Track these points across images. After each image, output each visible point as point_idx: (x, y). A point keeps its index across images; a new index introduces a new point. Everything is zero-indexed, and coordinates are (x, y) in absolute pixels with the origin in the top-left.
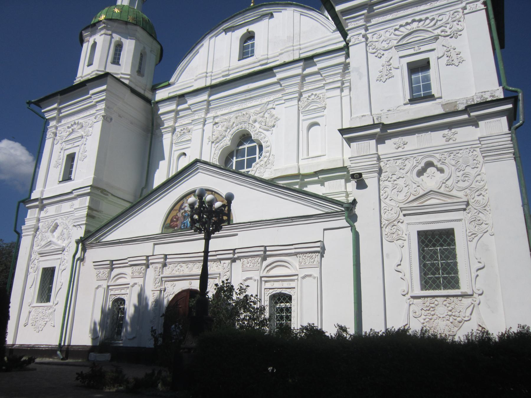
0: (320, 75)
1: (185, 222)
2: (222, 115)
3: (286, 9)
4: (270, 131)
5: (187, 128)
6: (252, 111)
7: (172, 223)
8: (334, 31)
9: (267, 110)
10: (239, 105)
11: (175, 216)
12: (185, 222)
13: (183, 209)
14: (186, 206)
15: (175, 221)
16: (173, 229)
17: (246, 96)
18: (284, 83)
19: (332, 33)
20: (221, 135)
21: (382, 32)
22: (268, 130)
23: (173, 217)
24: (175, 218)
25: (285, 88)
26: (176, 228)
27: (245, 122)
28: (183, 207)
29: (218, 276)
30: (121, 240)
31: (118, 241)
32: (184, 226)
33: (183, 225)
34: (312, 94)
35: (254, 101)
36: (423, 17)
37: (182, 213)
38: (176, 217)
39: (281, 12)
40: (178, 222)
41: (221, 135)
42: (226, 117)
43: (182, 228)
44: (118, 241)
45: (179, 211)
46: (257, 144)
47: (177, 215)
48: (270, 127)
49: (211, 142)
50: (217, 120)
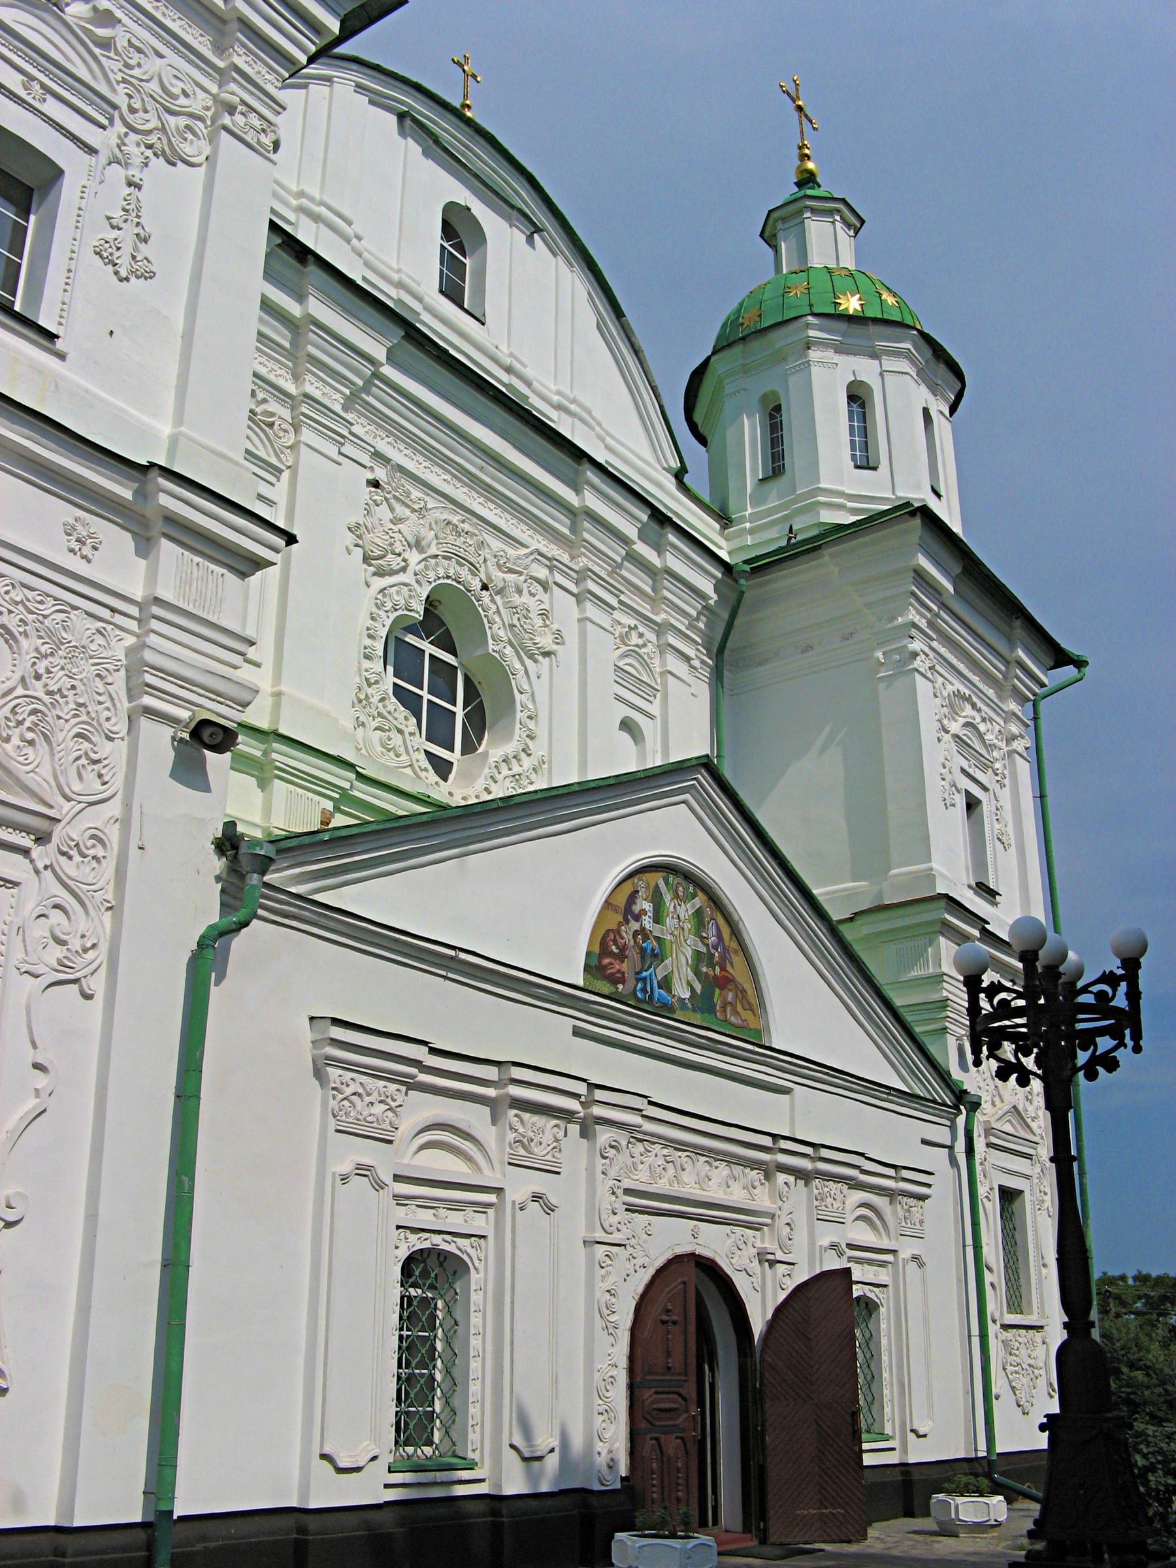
0: (650, 582)
1: (645, 974)
2: (401, 469)
3: (572, 266)
4: (536, 661)
5: (265, 401)
6: (496, 544)
7: (606, 961)
8: (668, 470)
9: (532, 578)
10: (448, 477)
11: (612, 930)
12: (645, 974)
13: (637, 918)
14: (644, 912)
15: (611, 954)
16: (612, 989)
17: (481, 469)
18: (590, 533)
19: (664, 469)
20: (399, 555)
21: (940, 680)
22: (531, 657)
23: (608, 931)
24: (615, 943)
25: (584, 547)
26: (620, 987)
27: (474, 570)
28: (636, 909)
29: (768, 1221)
30: (463, 956)
31: (452, 953)
32: (644, 990)
33: (639, 986)
34: (636, 627)
35: (492, 506)
36: (979, 704)
37: (636, 933)
38: (618, 937)
39: (555, 255)
40: (625, 966)
41: (399, 555)
42: (416, 494)
43: (639, 995)
44: (452, 953)
45: (627, 922)
46: (460, 663)
47: (618, 932)
48: (539, 648)
49: (358, 553)
50: (381, 474)
